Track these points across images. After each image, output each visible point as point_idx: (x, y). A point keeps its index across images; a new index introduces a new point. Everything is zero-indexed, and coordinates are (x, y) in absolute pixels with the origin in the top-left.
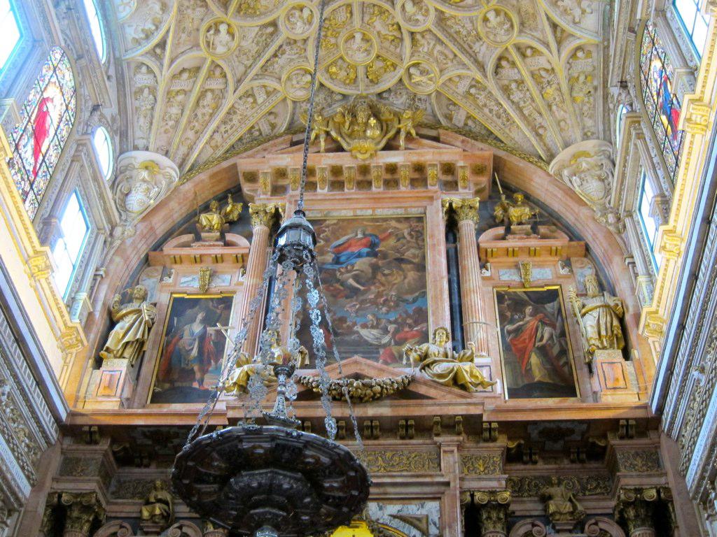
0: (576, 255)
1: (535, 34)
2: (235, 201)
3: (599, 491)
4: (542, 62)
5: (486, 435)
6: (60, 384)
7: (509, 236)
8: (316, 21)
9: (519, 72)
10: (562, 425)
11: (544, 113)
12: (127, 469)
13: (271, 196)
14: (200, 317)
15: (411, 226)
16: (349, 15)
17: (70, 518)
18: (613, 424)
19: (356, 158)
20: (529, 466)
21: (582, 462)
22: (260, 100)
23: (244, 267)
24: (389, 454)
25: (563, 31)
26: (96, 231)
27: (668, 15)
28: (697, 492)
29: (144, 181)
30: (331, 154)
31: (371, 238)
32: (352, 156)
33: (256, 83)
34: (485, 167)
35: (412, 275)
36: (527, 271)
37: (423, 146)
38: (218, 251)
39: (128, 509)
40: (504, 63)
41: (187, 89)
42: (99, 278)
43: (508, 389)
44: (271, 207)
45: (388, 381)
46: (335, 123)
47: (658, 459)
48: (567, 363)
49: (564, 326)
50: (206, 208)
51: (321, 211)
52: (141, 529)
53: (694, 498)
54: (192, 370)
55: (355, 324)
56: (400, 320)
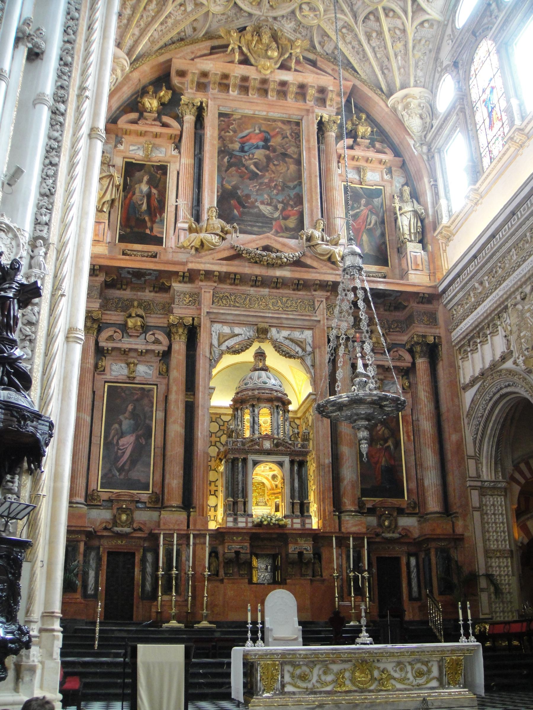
3: (398, 329)
7: (356, 147)
9: (381, 26)
10: (387, 292)
14: (146, 179)
15: (291, 128)
19: (260, 72)
21: (392, 311)
22: (189, 9)
24: (284, 299)
30: (242, 66)
31: (264, 134)
32: (257, 70)
35: (293, 167)
36: (365, 174)
39: (114, 318)
40: (372, 17)
45: (291, 256)
48: (384, 243)
51: (230, 107)
52: (127, 333)
53: (455, 346)
55: (256, 201)
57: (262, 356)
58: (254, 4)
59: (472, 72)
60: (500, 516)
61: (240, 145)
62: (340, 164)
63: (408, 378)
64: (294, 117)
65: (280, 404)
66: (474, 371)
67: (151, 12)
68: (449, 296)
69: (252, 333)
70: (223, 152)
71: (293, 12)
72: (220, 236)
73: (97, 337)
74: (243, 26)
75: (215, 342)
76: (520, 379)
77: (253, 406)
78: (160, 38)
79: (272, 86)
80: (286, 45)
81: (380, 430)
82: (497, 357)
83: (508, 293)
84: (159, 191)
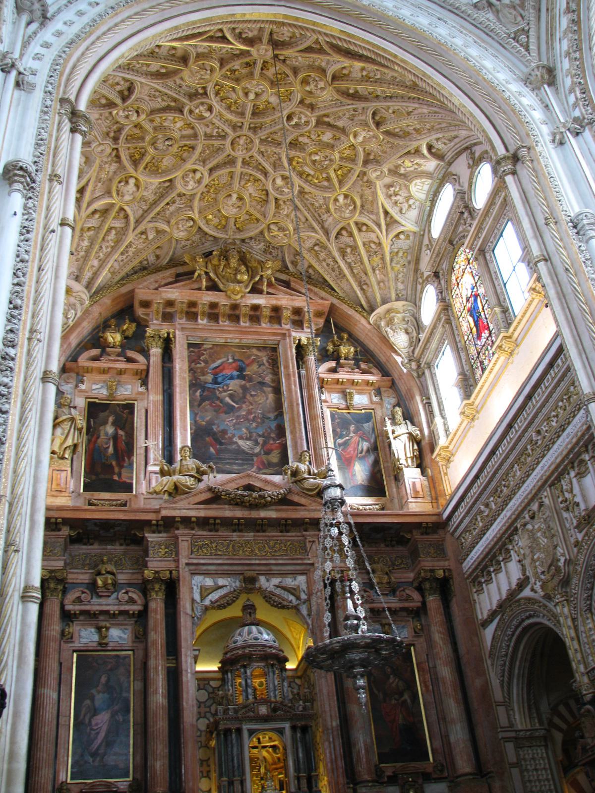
1: (371, 216)
3: (403, 566)
4: (373, 237)
7: (339, 369)
9: (355, 240)
12: (76, 546)
14: (111, 419)
15: (268, 355)
18: (418, 525)
19: (230, 297)
21: (393, 546)
22: (151, 237)
24: (272, 543)
25: (392, 217)
27: (488, 258)
31: (239, 363)
32: (226, 295)
33: (152, 225)
36: (351, 398)
38: (122, 365)
39: (82, 577)
40: (344, 233)
45: (275, 493)
48: (380, 471)
53: (468, 578)
54: (111, 464)
55: (234, 436)
57: (251, 609)
59: (454, 281)
60: (544, 772)
62: (323, 389)
63: (419, 620)
64: (270, 342)
65: (275, 662)
66: (491, 604)
67: (110, 242)
68: (454, 523)
69: (238, 584)
70: (195, 385)
71: (262, 233)
72: (196, 477)
74: (209, 250)
75: (197, 597)
76: (540, 607)
77: (245, 667)
78: (121, 268)
79: (243, 311)
80: (256, 267)
81: (393, 682)
82: (514, 586)
83: (516, 513)
84: (126, 433)
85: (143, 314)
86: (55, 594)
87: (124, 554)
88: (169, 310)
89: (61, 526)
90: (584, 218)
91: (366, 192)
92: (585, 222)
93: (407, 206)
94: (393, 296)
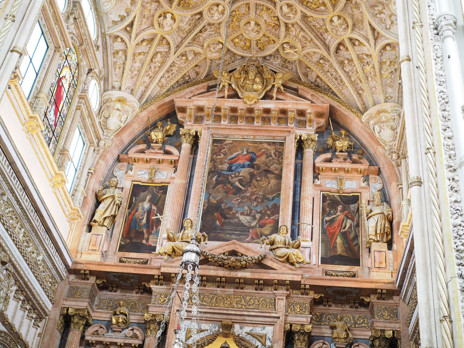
0: (373, 173)
1: (361, 32)
2: (172, 123)
5: (303, 291)
6: (67, 244)
8: (227, 13)
10: (346, 289)
11: (363, 81)
12: (104, 292)
13: (194, 123)
14: (148, 198)
15: (276, 148)
16: (247, 9)
17: (73, 322)
18: (374, 291)
19: (246, 103)
20: (327, 307)
21: (357, 308)
22: (190, 58)
23: (176, 167)
24: (248, 298)
25: (378, 33)
26: (89, 144)
28: (412, 338)
29: (118, 110)
31: (251, 155)
32: (243, 101)
33: (187, 49)
34: (324, 114)
35: (273, 182)
37: (288, 97)
38: (161, 157)
39: (104, 315)
40: (341, 47)
41: (145, 51)
42: (90, 174)
43: (321, 258)
44: (193, 132)
46: (235, 78)
47: (397, 312)
48: (357, 244)
49: (359, 220)
50: (154, 126)
51: (223, 135)
52: (111, 329)
56: (263, 212)
58: (245, 48)
61: (228, 165)
62: (320, 176)
67: (157, 63)
70: (211, 172)
73: (84, 332)
85: (180, 117)
86: (77, 327)
87: (139, 300)
88: (200, 114)
89: (89, 276)
90: (443, 19)
91: (355, 13)
92: (443, 23)
93: (390, 22)
94: (382, 98)
